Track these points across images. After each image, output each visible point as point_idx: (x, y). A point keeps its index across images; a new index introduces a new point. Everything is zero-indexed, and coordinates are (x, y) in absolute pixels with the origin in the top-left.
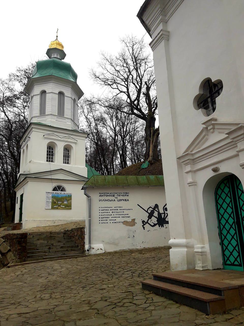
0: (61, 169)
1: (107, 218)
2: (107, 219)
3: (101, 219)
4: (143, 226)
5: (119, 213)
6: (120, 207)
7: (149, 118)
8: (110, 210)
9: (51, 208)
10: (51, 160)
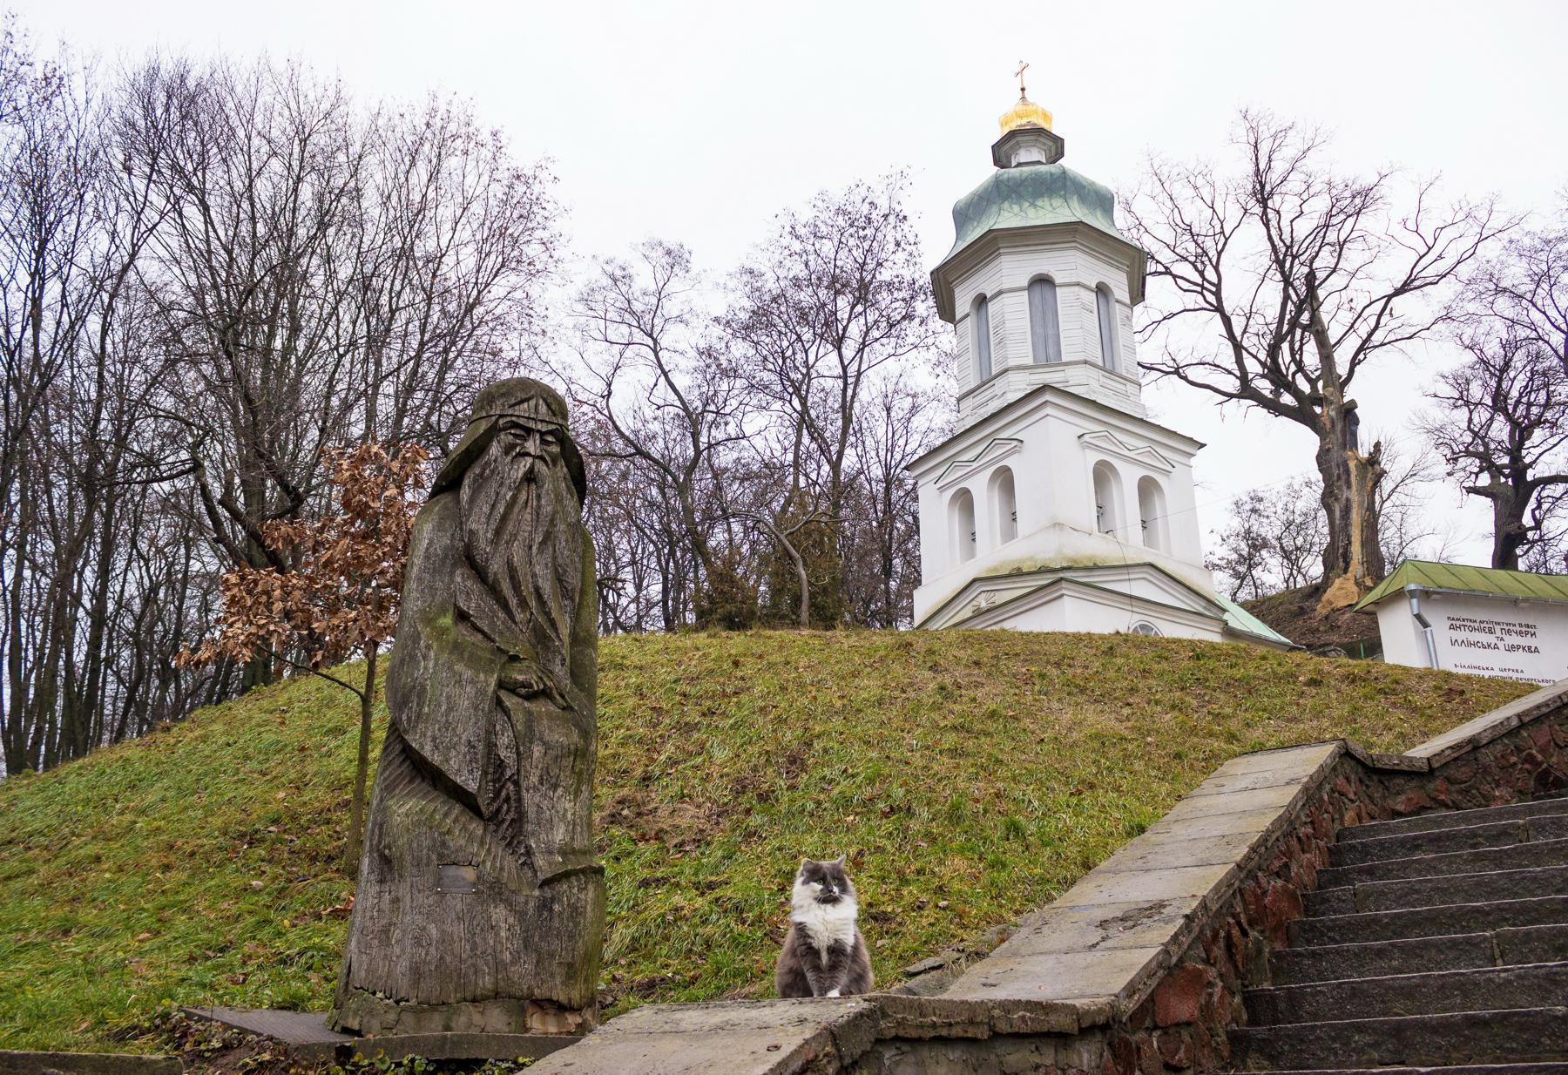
7: (1333, 413)
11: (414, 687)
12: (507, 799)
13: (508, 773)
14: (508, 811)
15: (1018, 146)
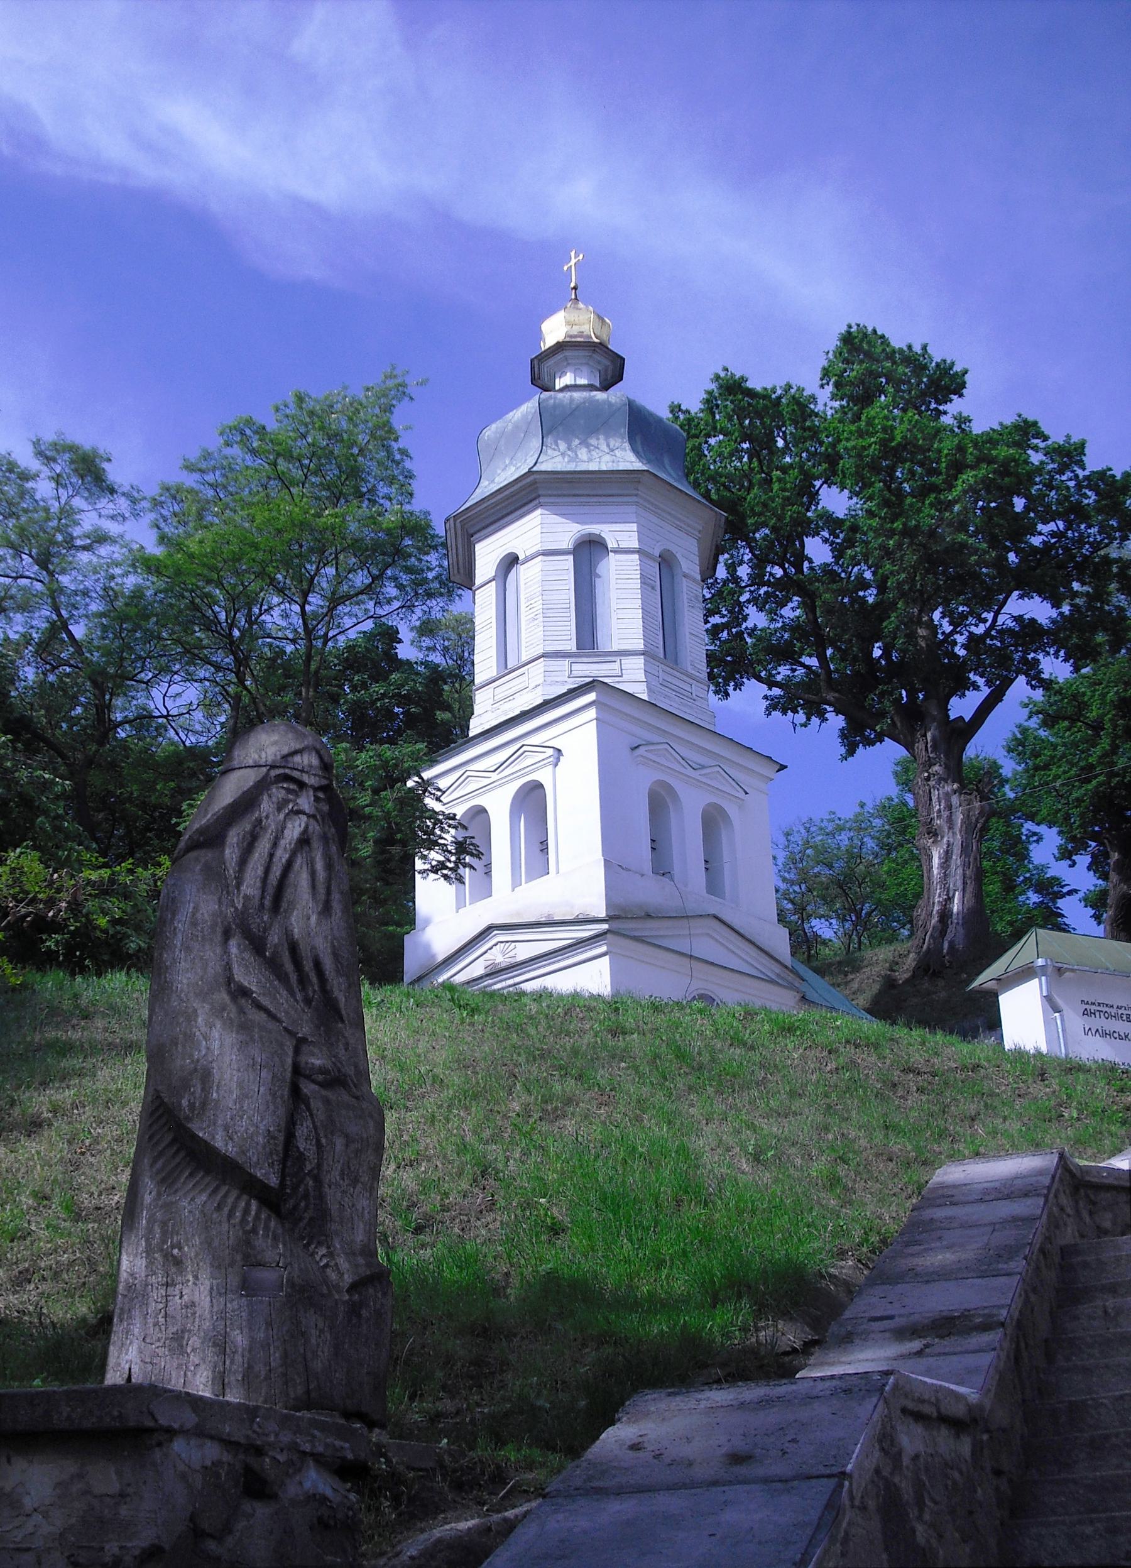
0: (716, 917)
11: (196, 1070)
12: (306, 1196)
13: (308, 1167)
14: (307, 1206)
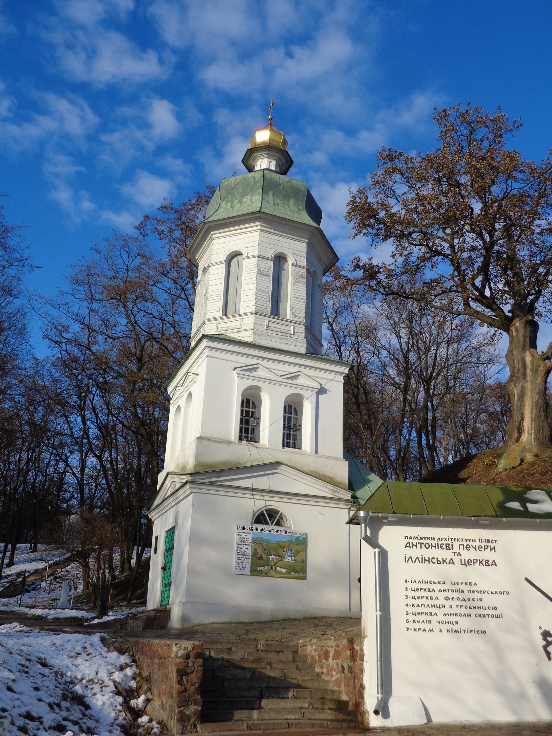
1: (431, 614)
2: (429, 618)
3: (411, 617)
4: (545, 648)
5: (468, 604)
6: (470, 584)
8: (440, 591)
9: (251, 571)
10: (250, 435)
15: (255, 159)
